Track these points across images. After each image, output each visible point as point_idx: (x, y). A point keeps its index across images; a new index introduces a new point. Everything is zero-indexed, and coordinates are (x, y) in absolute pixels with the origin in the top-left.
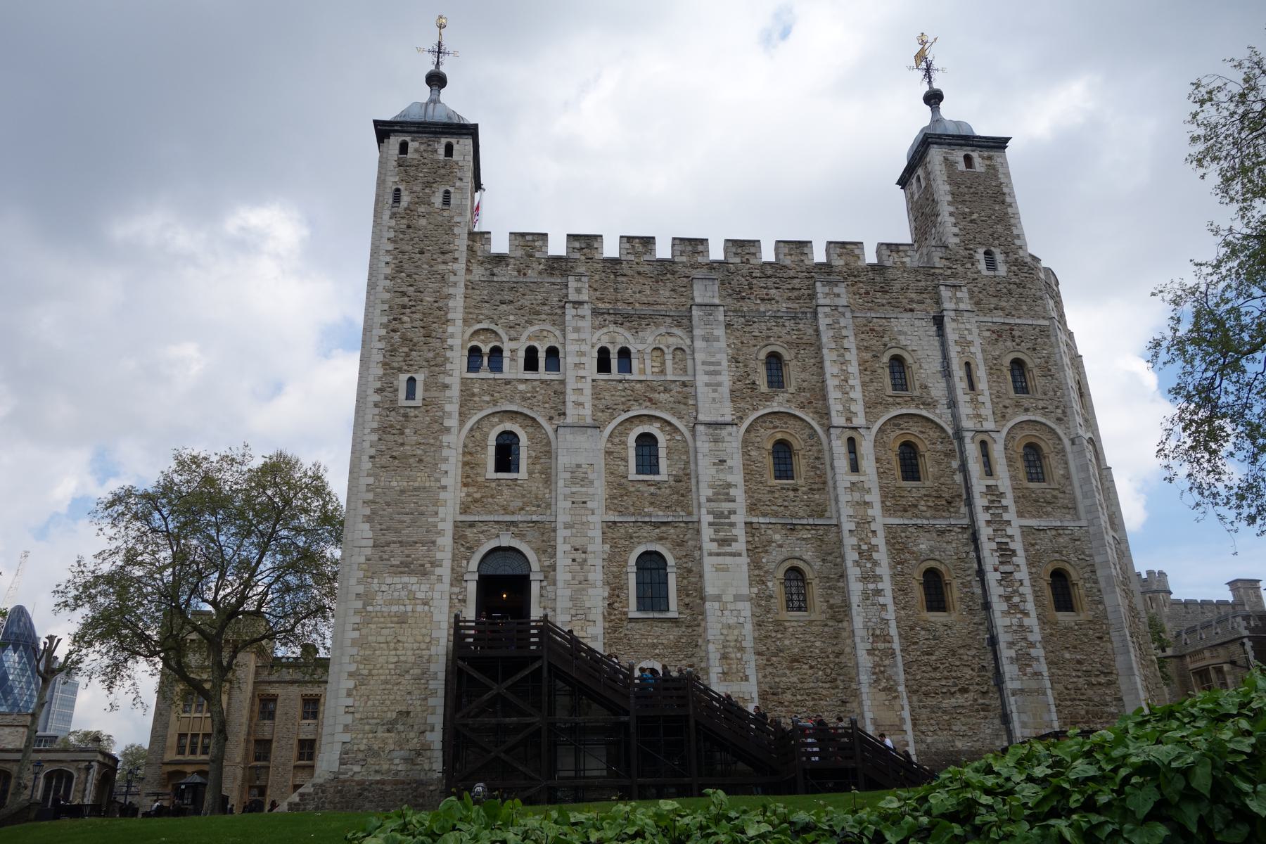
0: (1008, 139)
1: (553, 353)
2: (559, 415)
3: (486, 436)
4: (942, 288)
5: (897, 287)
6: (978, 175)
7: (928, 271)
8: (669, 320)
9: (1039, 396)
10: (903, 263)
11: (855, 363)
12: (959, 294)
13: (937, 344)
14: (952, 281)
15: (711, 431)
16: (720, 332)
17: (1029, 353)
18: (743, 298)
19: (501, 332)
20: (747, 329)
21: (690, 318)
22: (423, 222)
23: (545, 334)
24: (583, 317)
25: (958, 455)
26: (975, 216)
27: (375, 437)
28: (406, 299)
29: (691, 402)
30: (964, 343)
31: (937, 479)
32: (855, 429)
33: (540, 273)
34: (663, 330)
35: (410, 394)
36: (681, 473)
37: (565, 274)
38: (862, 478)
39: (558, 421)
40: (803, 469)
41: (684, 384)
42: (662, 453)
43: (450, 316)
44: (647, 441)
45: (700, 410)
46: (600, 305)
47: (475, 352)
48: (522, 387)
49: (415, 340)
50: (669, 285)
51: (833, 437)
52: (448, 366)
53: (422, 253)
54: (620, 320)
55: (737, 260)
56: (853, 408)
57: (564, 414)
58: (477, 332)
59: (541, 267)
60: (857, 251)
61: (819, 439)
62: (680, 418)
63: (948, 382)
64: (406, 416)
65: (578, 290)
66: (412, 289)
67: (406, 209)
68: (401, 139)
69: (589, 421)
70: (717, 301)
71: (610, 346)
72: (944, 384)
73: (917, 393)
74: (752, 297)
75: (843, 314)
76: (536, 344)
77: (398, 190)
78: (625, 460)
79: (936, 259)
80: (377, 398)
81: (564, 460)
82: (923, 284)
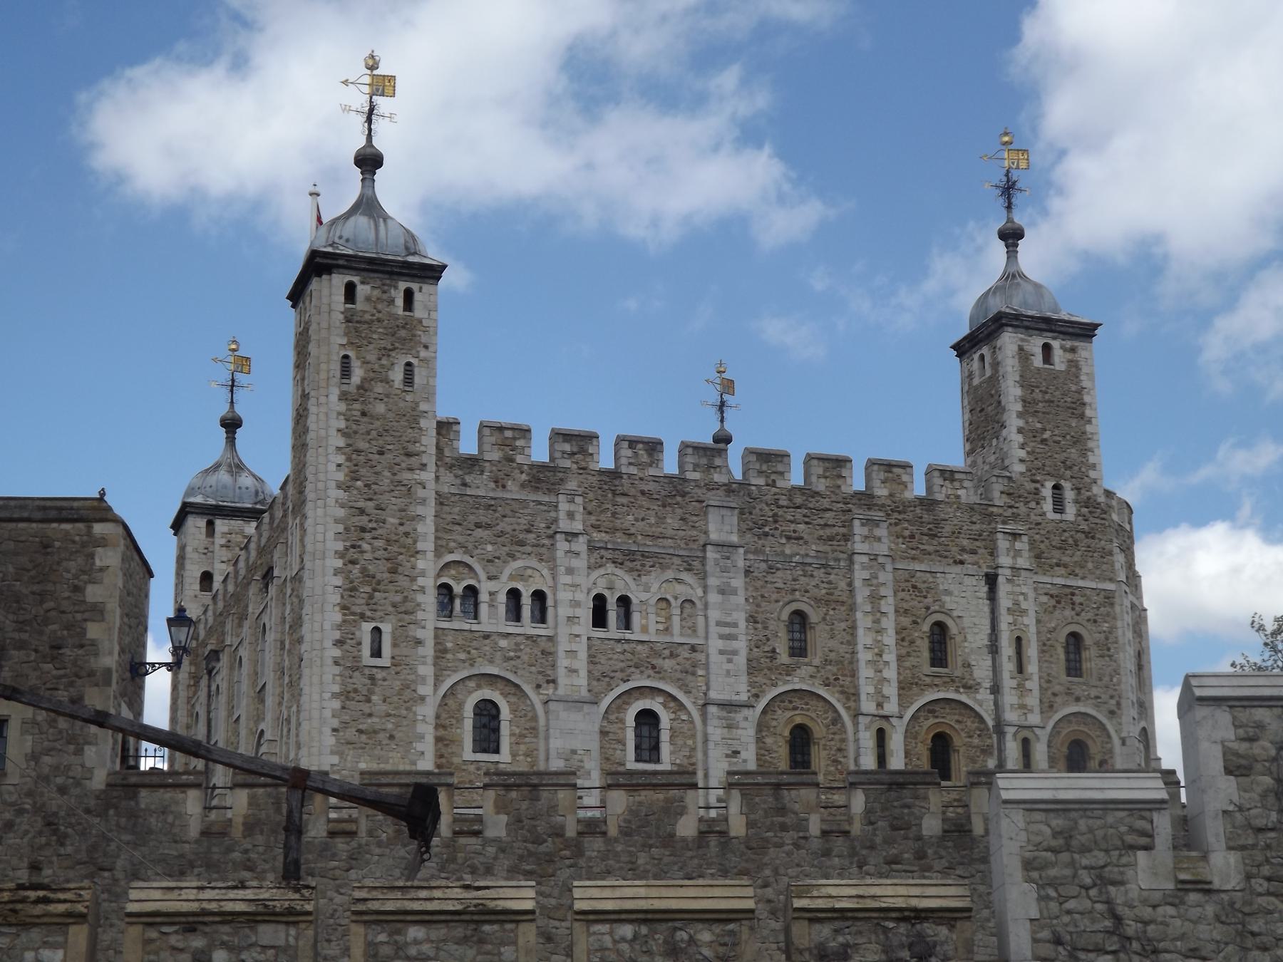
0: (1096, 326)
1: (539, 596)
2: (548, 682)
3: (461, 706)
4: (1000, 536)
5: (948, 529)
6: (1055, 375)
7: (984, 511)
8: (677, 561)
9: (1094, 682)
10: (958, 497)
11: (891, 632)
12: (1018, 545)
13: (987, 609)
14: (1010, 527)
15: (724, 714)
16: (738, 582)
17: (1089, 625)
18: (766, 534)
19: (477, 567)
20: (769, 578)
21: (703, 560)
22: (380, 408)
23: (529, 572)
24: (578, 554)
25: (996, 752)
26: (1047, 435)
27: (336, 704)
28: (365, 518)
29: (700, 672)
30: (1016, 610)
32: (886, 718)
33: (523, 486)
34: (670, 574)
35: (377, 653)
36: (685, 762)
37: (553, 489)
40: (822, 764)
41: (693, 649)
42: (665, 736)
43: (420, 546)
44: (647, 719)
45: (713, 684)
47: (445, 590)
48: (503, 643)
49: (379, 576)
50: (679, 511)
51: (861, 727)
53: (381, 453)
54: (620, 558)
55: (761, 481)
57: (554, 681)
58: (447, 565)
59: (524, 477)
60: (905, 478)
61: (843, 725)
62: (688, 692)
63: (994, 660)
64: (372, 678)
65: (571, 515)
66: (370, 504)
67: (360, 387)
68: (348, 278)
70: (734, 539)
71: (607, 593)
72: (989, 663)
73: (958, 673)
75: (883, 566)
76: (520, 586)
77: (346, 357)
78: (622, 742)
79: (996, 494)
80: (337, 652)
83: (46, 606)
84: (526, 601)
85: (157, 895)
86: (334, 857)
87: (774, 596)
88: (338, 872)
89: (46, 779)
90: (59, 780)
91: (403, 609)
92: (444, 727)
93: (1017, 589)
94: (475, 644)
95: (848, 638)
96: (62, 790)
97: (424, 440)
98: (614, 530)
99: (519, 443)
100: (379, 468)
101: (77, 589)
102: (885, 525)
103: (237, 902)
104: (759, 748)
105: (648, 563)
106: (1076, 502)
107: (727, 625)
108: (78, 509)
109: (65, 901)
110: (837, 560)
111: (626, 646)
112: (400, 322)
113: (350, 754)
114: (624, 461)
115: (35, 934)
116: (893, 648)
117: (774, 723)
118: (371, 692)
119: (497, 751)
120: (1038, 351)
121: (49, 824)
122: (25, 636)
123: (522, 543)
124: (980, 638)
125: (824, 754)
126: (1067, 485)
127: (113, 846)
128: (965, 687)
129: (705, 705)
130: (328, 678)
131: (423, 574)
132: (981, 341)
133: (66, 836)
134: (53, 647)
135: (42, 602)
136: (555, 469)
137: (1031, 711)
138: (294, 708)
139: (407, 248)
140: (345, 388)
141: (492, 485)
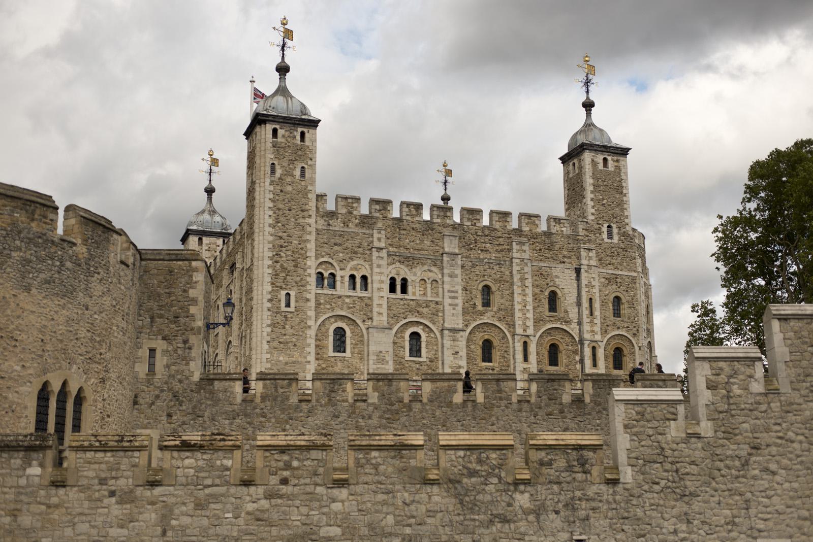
0: (629, 149)
1: (364, 278)
2: (368, 319)
3: (328, 330)
4: (582, 250)
5: (557, 246)
6: (610, 173)
8: (429, 261)
10: (562, 231)
11: (530, 295)
12: (591, 254)
13: (576, 285)
14: (587, 246)
16: (458, 271)
18: (471, 249)
19: (335, 264)
20: (472, 270)
22: (289, 188)
24: (382, 258)
26: (605, 202)
27: (269, 329)
28: (283, 241)
29: (440, 314)
30: (590, 286)
31: (567, 366)
32: (528, 336)
33: (356, 225)
34: (426, 267)
35: (288, 305)
36: (433, 357)
37: (371, 226)
38: (529, 366)
39: (369, 323)
40: (498, 358)
41: (437, 303)
42: (423, 345)
43: (308, 254)
44: (415, 336)
45: (446, 320)
46: (391, 249)
48: (347, 300)
49: (289, 269)
51: (516, 341)
52: (308, 287)
53: (290, 210)
54: (402, 260)
55: (469, 223)
56: (527, 324)
57: (371, 319)
58: (321, 263)
59: (357, 221)
60: (537, 222)
61: (508, 340)
62: (434, 324)
63: (579, 309)
64: (286, 317)
65: (379, 240)
67: (280, 179)
68: (274, 126)
69: (386, 324)
70: (457, 251)
71: (396, 277)
72: (577, 310)
73: (562, 315)
74: (477, 248)
75: (526, 264)
76: (355, 273)
78: (403, 347)
79: (580, 230)
80: (269, 305)
81: (373, 348)
82: (572, 245)
83: (171, 298)
84: (358, 280)
85: (269, 438)
86: (301, 411)
87: (475, 278)
88: (303, 418)
89: (173, 376)
90: (179, 377)
91: (300, 284)
92: (320, 340)
93: (590, 275)
94: (334, 300)
95: (510, 298)
96: (180, 381)
97: (310, 204)
98: (400, 246)
99: (355, 205)
100: (289, 217)
101: (185, 291)
102: (528, 244)
103: (301, 441)
104: (467, 350)
105: (416, 262)
106: (618, 234)
107: (453, 292)
108: (185, 254)
109: (232, 440)
110: (505, 261)
111: (405, 302)
112: (298, 147)
113: (275, 353)
114: (404, 214)
115: (220, 454)
116: (531, 303)
117: (475, 339)
118: (285, 324)
119: (344, 351)
120: (601, 161)
121: (175, 396)
122: (162, 312)
123: (356, 253)
124: (572, 298)
125: (498, 353)
126: (614, 226)
127: (203, 406)
128: (565, 322)
129: (442, 330)
130: (265, 317)
131: (310, 267)
132: (573, 156)
133: (182, 402)
134: (175, 317)
135: (170, 297)
136: (372, 217)
137: (597, 334)
138: (248, 331)
139: (302, 112)
140: (273, 179)
141: (342, 225)
